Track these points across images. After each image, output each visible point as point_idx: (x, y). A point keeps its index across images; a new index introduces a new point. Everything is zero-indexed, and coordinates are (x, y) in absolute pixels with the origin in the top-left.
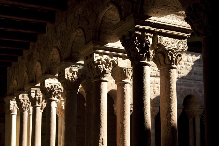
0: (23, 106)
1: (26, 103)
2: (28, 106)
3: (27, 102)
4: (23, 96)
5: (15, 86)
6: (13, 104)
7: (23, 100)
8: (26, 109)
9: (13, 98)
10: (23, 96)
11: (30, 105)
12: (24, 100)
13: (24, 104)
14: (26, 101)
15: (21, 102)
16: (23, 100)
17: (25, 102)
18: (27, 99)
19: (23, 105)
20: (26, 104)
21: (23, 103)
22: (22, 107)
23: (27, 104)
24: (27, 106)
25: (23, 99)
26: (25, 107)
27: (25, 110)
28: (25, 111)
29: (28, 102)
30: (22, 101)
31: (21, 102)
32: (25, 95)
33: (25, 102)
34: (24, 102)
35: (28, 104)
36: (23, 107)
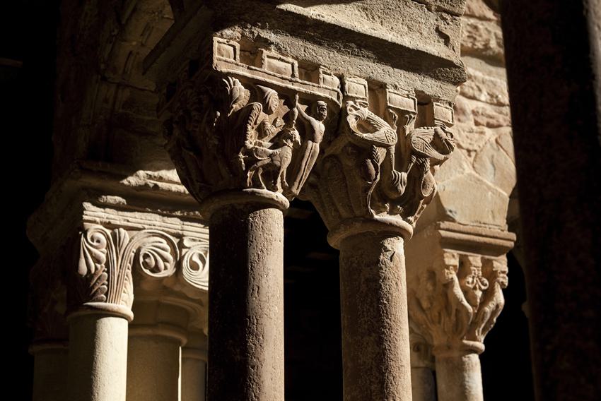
0: (251, 142)
1: (281, 122)
2: (299, 152)
3: (288, 118)
4: (251, 53)
5: (125, 94)
6: (109, 232)
7: (251, 84)
9: (111, 184)
10: (251, 53)
11: (314, 147)
12: (257, 90)
13: (261, 131)
14: (272, 94)
15: (236, 107)
16: (251, 84)
17: (267, 110)
18: (290, 86)
20: (273, 130)
21: (248, 110)
24: (287, 153)
26: (267, 161)
29: (295, 110)
30: (242, 93)
31: (230, 98)
32: (267, 44)
33: (267, 110)
34: (258, 106)
35: (296, 134)
36: (249, 152)
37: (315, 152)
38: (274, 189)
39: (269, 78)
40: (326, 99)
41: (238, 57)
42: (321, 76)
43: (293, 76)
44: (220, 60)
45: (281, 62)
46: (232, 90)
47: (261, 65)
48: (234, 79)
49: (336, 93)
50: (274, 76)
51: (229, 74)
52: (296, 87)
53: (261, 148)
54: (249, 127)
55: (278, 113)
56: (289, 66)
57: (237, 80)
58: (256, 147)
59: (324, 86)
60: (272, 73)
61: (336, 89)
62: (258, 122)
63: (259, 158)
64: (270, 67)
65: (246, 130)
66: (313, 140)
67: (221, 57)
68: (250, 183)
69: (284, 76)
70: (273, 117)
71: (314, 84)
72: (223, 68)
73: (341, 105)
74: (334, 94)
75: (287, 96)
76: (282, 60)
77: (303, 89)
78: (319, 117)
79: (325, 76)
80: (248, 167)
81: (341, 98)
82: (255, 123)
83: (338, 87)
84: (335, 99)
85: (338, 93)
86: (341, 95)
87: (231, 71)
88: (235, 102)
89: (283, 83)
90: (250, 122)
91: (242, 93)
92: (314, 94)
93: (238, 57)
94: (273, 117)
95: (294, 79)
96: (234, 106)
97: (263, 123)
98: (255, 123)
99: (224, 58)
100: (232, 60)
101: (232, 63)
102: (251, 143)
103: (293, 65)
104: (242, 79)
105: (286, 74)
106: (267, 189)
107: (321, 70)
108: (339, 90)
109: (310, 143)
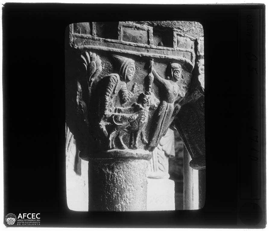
2: (155, 114)
8: (132, 145)
11: (170, 106)
14: (130, 64)
17: (124, 78)
18: (145, 54)
19: (111, 108)
21: (105, 82)
22: (103, 124)
23: (141, 99)
25: (105, 48)
27: (127, 150)
28: (133, 158)
29: (151, 75)
30: (99, 64)
31: (89, 72)
33: (124, 78)
34: (115, 76)
37: (170, 111)
38: (135, 148)
39: (124, 48)
40: (180, 62)
41: (95, 32)
42: (175, 40)
43: (149, 43)
44: (76, 36)
45: (136, 31)
46: (89, 65)
47: (116, 37)
48: (91, 53)
49: (190, 54)
50: (130, 45)
51: (85, 49)
52: (151, 54)
53: (121, 114)
54: (107, 98)
55: (135, 79)
56: (144, 34)
57: (94, 55)
58: (117, 114)
59: (178, 48)
60: (128, 43)
61: (190, 50)
62: (117, 92)
63: (118, 124)
64: (126, 37)
65: (104, 101)
66: (168, 100)
67: (77, 34)
68: (112, 145)
69: (139, 44)
70: (130, 84)
71: (168, 48)
72: (80, 46)
73: (193, 65)
74: (187, 55)
75: (145, 62)
76: (138, 29)
77: (158, 55)
78: (174, 79)
79: (179, 37)
80: (110, 132)
81: (194, 59)
82: (114, 93)
83: (192, 48)
84: (188, 61)
85: (192, 54)
86: (194, 55)
87: (87, 46)
88: (93, 76)
89: (138, 51)
90: (108, 94)
91: (99, 64)
92: (168, 58)
93: (95, 32)
94: (130, 84)
95: (149, 46)
96: (93, 80)
97: (121, 92)
98: (114, 93)
99: (80, 35)
100: (90, 36)
101: (89, 38)
102: (111, 111)
103: (148, 31)
104: (101, 53)
105: (141, 42)
106: (130, 148)
107: (175, 34)
108: (193, 51)
109: (165, 103)
